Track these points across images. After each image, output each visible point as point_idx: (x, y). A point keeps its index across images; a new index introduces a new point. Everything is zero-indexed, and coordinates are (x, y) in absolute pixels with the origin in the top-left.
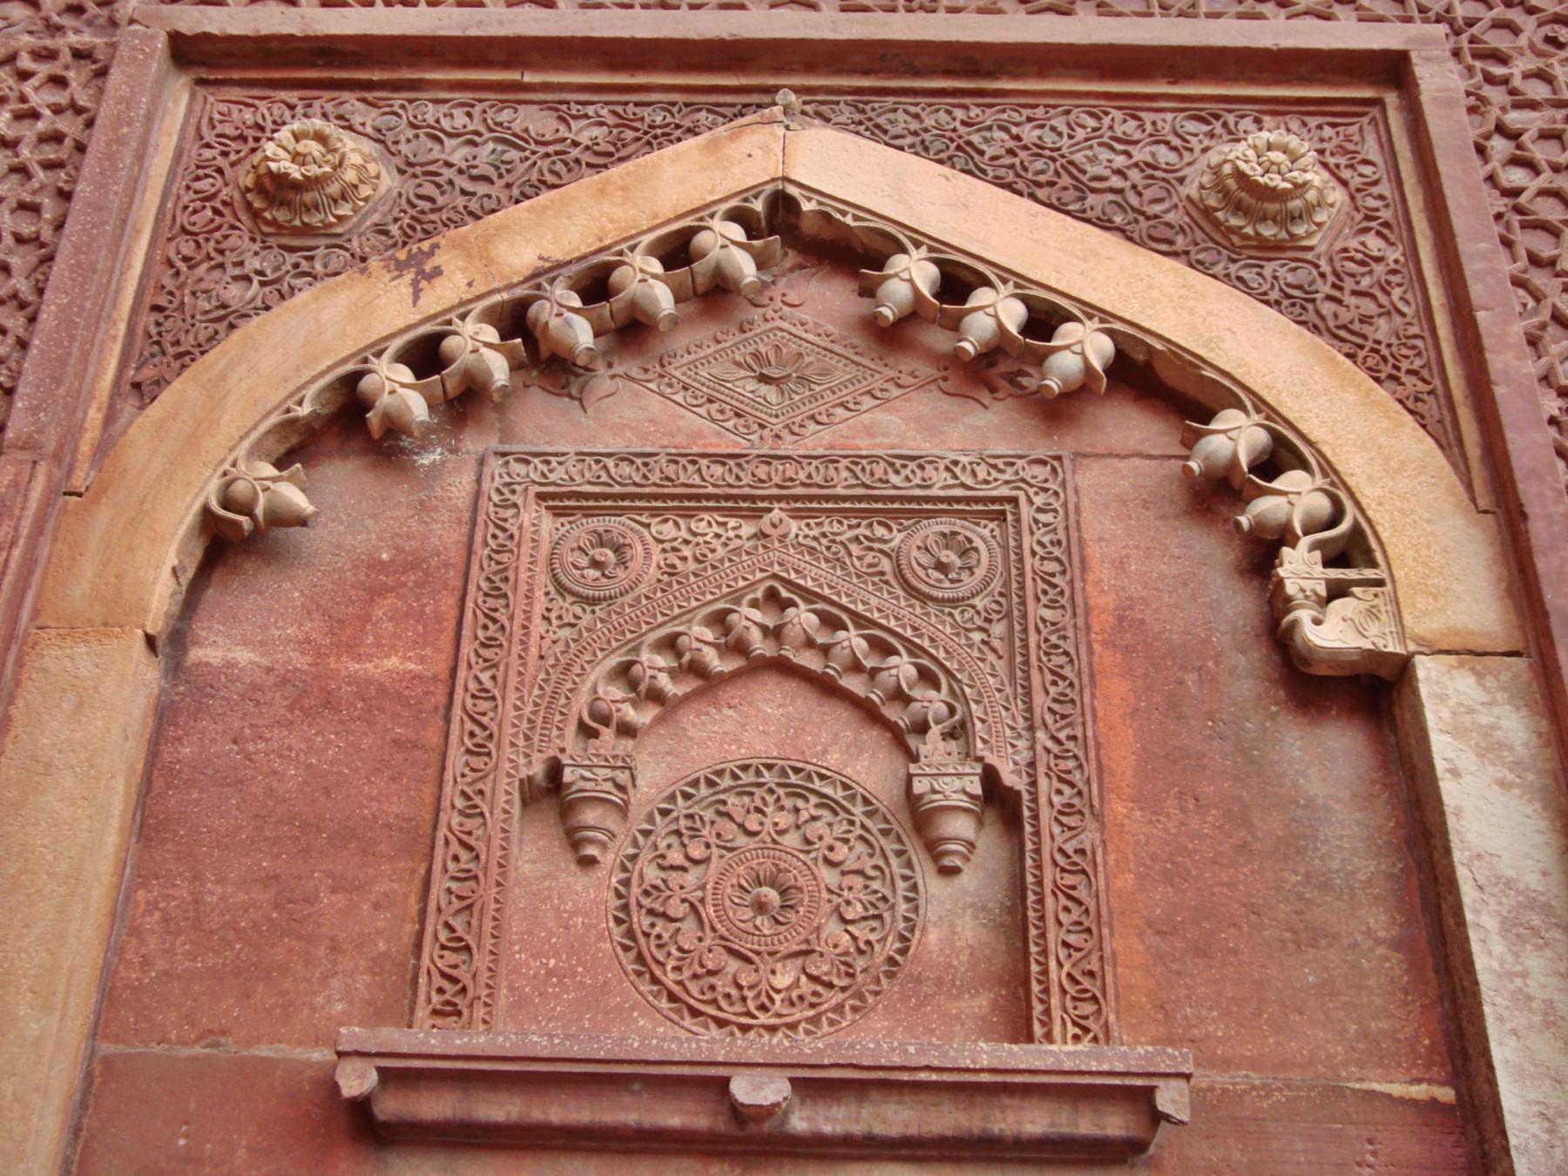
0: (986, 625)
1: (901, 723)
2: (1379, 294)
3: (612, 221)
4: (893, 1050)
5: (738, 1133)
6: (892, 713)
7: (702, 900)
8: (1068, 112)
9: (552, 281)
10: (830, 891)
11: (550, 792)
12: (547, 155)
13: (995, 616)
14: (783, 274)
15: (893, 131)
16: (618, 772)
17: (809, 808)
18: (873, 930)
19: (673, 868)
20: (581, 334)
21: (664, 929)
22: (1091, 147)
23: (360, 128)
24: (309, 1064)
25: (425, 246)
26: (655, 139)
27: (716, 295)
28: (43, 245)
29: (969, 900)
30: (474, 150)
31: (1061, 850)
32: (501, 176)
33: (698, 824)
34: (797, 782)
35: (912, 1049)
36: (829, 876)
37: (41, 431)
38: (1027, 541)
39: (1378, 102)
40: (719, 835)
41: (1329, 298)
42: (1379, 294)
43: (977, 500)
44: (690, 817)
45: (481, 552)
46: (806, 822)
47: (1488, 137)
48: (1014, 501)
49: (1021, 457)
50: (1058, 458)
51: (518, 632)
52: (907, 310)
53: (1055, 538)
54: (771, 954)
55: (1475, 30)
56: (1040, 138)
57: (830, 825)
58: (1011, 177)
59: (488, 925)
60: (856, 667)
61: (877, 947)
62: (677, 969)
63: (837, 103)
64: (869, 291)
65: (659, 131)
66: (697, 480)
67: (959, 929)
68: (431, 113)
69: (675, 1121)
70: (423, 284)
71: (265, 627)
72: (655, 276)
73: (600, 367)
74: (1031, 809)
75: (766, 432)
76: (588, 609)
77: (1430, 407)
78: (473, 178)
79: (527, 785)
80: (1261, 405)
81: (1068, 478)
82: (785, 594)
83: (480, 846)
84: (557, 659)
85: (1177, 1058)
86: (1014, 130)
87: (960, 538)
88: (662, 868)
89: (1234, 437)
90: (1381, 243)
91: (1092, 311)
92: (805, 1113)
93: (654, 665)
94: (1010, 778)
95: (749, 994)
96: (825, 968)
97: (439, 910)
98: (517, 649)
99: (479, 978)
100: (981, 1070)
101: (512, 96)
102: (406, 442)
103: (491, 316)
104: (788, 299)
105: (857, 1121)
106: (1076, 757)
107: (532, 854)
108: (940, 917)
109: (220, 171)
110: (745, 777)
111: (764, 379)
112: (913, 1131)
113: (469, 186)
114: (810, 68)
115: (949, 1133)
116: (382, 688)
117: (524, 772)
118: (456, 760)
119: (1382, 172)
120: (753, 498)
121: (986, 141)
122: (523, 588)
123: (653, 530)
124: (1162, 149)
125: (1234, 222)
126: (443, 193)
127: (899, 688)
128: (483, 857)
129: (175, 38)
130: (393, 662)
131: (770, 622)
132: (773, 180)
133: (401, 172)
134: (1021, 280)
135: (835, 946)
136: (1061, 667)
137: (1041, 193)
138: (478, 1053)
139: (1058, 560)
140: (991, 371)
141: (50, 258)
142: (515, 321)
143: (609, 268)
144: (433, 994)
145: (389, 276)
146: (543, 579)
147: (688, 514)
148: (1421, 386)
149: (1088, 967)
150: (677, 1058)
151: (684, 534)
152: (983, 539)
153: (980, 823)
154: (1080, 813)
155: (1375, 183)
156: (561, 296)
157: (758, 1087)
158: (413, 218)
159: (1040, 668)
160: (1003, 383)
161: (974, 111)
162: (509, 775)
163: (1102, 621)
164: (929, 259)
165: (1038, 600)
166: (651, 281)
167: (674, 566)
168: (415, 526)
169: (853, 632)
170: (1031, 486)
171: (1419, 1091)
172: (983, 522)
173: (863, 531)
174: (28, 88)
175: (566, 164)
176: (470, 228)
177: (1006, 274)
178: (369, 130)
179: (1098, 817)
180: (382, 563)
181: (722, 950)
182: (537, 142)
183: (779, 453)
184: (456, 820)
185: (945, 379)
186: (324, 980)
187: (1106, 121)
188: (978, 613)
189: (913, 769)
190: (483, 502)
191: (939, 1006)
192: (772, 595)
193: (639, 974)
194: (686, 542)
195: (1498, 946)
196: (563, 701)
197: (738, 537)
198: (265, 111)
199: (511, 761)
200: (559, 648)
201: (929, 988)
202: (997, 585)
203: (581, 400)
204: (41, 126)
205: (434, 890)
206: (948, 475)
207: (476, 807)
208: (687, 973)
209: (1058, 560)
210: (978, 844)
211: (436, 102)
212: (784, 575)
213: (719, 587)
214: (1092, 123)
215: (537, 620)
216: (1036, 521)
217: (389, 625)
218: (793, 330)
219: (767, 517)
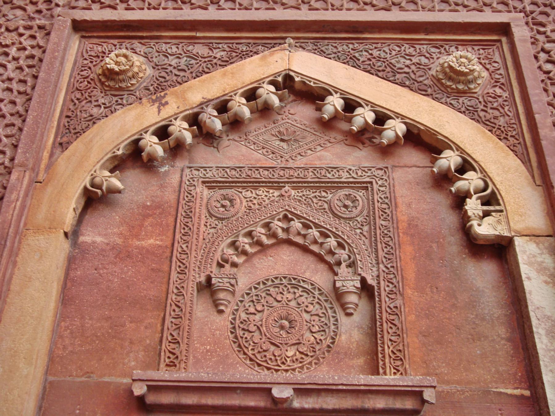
0: (361, 227)
1: (332, 262)
2: (500, 109)
3: (228, 85)
4: (330, 378)
5: (274, 407)
6: (329, 258)
7: (261, 325)
8: (389, 45)
9: (207, 106)
10: (307, 322)
12: (205, 62)
13: (365, 224)
14: (289, 103)
15: (327, 52)
16: (231, 280)
17: (299, 292)
18: (322, 335)
19: (251, 314)
20: (217, 125)
21: (248, 335)
22: (397, 58)
23: (139, 53)
24: (122, 384)
25: (162, 94)
26: (243, 56)
27: (265, 111)
28: (27, 95)
29: (356, 324)
30: (179, 60)
31: (389, 307)
32: (189, 69)
33: (260, 298)
34: (295, 283)
35: (336, 378)
36: (306, 316)
37: (27, 160)
38: (376, 197)
39: (499, 41)
40: (267, 302)
41: (482, 110)
42: (500, 109)
43: (358, 183)
44: (257, 295)
45: (182, 202)
46: (298, 297)
47: (538, 53)
48: (371, 183)
49: (374, 167)
50: (387, 168)
51: (196, 230)
52: (333, 116)
53: (386, 196)
54: (286, 344)
55: (533, 15)
56: (379, 54)
57: (307, 298)
58: (369, 68)
59: (186, 334)
60: (315, 242)
61: (324, 342)
62: (253, 349)
63: (308, 43)
64: (319, 109)
65: (245, 53)
66: (259, 176)
67: (353, 335)
68: (164, 47)
69: (252, 404)
70: (162, 107)
71: (106, 229)
72: (243, 104)
73: (224, 136)
74: (378, 292)
75: (283, 159)
76: (220, 222)
77: (519, 148)
78: (179, 70)
79: (199, 285)
80: (459, 148)
81: (390, 174)
82: (290, 216)
83: (183, 306)
84: (210, 240)
85: (431, 380)
86: (370, 52)
87: (352, 196)
88: (247, 314)
89: (449, 160)
90: (501, 91)
91: (398, 115)
92: (298, 401)
93: (244, 241)
94: (370, 281)
95: (278, 358)
96: (305, 349)
97: (168, 329)
98: (195, 236)
99: (182, 353)
100: (361, 385)
101: (193, 41)
102: (156, 163)
103: (185, 119)
104: (291, 112)
105: (317, 404)
106: (394, 274)
107: (201, 309)
108: (346, 331)
109: (90, 68)
110: (276, 281)
111: (282, 140)
112: (337, 407)
113: (177, 73)
114: (298, 30)
115: (350, 407)
116: (148, 251)
117: (198, 280)
118: (174, 276)
119: (501, 65)
120: (278, 183)
121: (360, 55)
122: (197, 215)
123: (243, 194)
124: (423, 58)
125: (449, 83)
126: (168, 75)
127: (331, 249)
128: (184, 310)
129: (74, 21)
130: (151, 241)
131: (285, 226)
132: (285, 70)
133: (154, 68)
134: (373, 105)
135: (309, 341)
136: (388, 242)
137: (380, 74)
138: (183, 380)
139: (387, 204)
141: (30, 99)
142: (194, 120)
143: (227, 101)
144: (166, 359)
145: (149, 105)
146: (204, 211)
147: (256, 188)
148: (516, 141)
149: (399, 348)
150: (253, 381)
151: (254, 195)
152: (360, 197)
153: (360, 297)
154: (395, 293)
155: (499, 69)
156: (210, 111)
157: (282, 391)
158: (158, 84)
159: (381, 242)
160: (368, 141)
161: (356, 45)
162: (193, 281)
163: (403, 225)
164: (340, 98)
165: (380, 218)
166: (242, 106)
167: (251, 207)
168: (159, 193)
169: (314, 230)
170: (377, 177)
171: (517, 392)
172: (360, 190)
173: (317, 194)
174: (22, 39)
175: (212, 65)
176: (178, 88)
177: (368, 102)
178: (142, 53)
179: (402, 295)
180: (148, 206)
181: (268, 343)
182: (201, 57)
183: (288, 166)
184: (174, 297)
185: (346, 140)
186: (128, 354)
187: (403, 48)
188: (359, 223)
189: (336, 278)
190: (183, 184)
191: (346, 362)
192: (285, 216)
193: (239, 351)
194: (255, 198)
195: (545, 340)
196: (212, 255)
197: (273, 196)
198: (106, 47)
199: (193, 276)
200: (210, 236)
201: (342, 356)
202: (365, 213)
203: (217, 148)
204: (27, 53)
205: (166, 322)
206: (348, 174)
207: (181, 292)
208: (256, 351)
209: (387, 204)
210: (359, 305)
211: (166, 43)
212: (290, 209)
213: (267, 214)
214: (398, 49)
215: (202, 226)
216: (379, 190)
217: (150, 228)
218: (292, 123)
219: (284, 189)
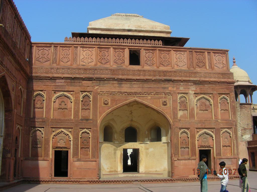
140: (65, 134)
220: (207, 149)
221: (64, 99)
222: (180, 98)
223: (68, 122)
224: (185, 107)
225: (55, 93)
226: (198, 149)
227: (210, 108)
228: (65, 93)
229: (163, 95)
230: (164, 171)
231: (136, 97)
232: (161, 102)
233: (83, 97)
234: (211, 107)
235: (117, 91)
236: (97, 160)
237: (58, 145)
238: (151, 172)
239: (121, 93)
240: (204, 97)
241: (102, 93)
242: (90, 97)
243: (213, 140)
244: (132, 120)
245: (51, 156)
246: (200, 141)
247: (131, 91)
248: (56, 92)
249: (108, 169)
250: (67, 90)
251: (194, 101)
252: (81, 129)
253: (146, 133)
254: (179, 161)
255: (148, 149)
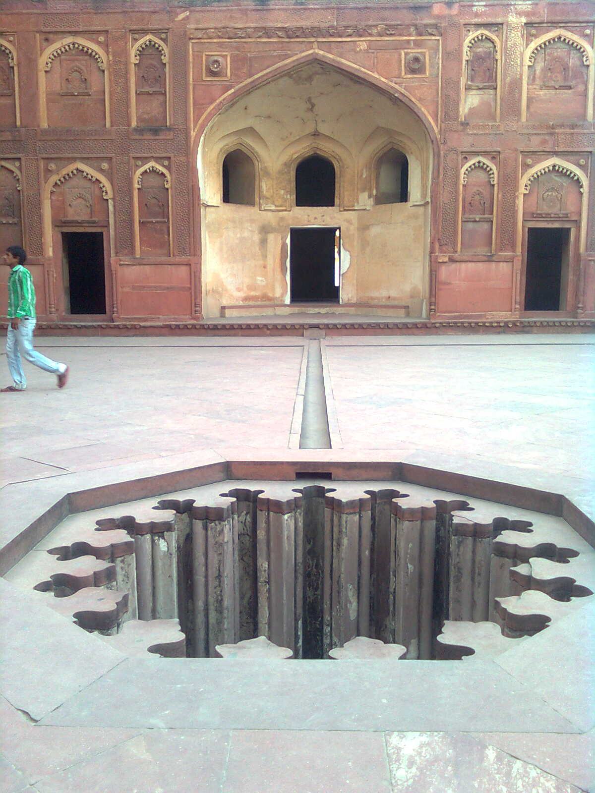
11: (70, 205)
107: (69, 208)
220: (557, 225)
221: (77, 60)
222: (470, 45)
223: (96, 138)
224: (490, 77)
225: (47, 40)
226: (523, 227)
227: (583, 78)
228: (82, 41)
229: (410, 35)
230: (412, 297)
231: (315, 45)
232: (403, 62)
233: (140, 51)
234: (585, 76)
235: (252, 25)
236: (193, 259)
237: (67, 217)
238: (376, 302)
239: (267, 32)
240: (562, 39)
241: (200, 36)
242: (163, 52)
243: (581, 194)
244: (316, 134)
245: (51, 249)
246: (534, 198)
247: (299, 24)
248: (51, 36)
249: (239, 290)
250: (86, 29)
251: (522, 54)
252: (139, 163)
253: (361, 176)
254: (454, 266)
255: (364, 228)
